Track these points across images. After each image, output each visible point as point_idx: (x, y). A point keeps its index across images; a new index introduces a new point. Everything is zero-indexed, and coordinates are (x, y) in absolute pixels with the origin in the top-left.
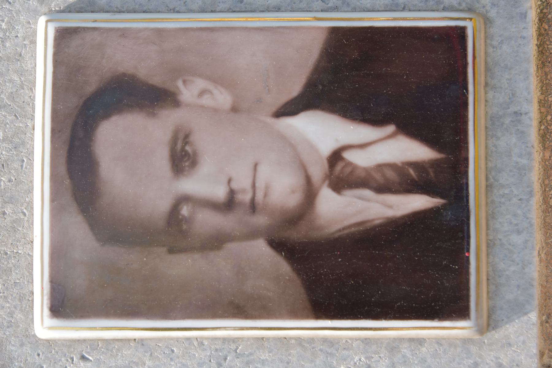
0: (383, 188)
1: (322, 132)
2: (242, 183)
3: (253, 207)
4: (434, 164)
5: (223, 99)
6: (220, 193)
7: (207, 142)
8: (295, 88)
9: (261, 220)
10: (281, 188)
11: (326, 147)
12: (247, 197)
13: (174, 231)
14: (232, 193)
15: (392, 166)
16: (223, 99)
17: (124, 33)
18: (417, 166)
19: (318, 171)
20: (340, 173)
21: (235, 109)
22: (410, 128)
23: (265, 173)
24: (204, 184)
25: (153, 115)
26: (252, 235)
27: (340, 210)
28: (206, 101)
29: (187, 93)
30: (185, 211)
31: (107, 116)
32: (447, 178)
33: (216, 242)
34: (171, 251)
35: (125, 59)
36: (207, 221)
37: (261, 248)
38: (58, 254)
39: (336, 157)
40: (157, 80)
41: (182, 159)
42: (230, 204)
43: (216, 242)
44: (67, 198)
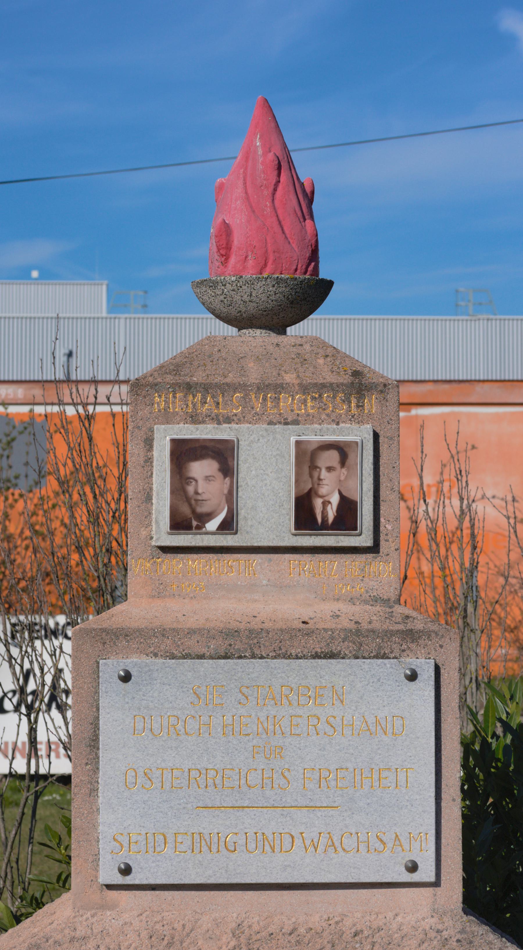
0: (323, 513)
1: (335, 499)
2: (324, 482)
3: (319, 484)
4: (328, 524)
5: (342, 478)
6: (322, 477)
7: (333, 474)
8: (344, 494)
9: (316, 486)
10: (323, 490)
11: (331, 500)
12: (321, 483)
13: (313, 467)
14: (321, 480)
15: (327, 515)
16: (342, 478)
17: (357, 456)
18: (327, 520)
19: (326, 498)
20: (326, 503)
21: (340, 481)
22: (336, 518)
23: (326, 487)
24: (324, 474)
25: (339, 462)
26: (313, 484)
27: (318, 503)
28: (342, 474)
29: (344, 470)
30: (318, 470)
31: (339, 453)
32: (324, 526)
33: (311, 476)
34: (309, 467)
35: (351, 457)
36: (316, 474)
37: (310, 486)
38: (309, 442)
39: (329, 502)
40: (347, 463)
41: (330, 469)
42: (319, 479)
43: (311, 476)
44: (321, 444)
